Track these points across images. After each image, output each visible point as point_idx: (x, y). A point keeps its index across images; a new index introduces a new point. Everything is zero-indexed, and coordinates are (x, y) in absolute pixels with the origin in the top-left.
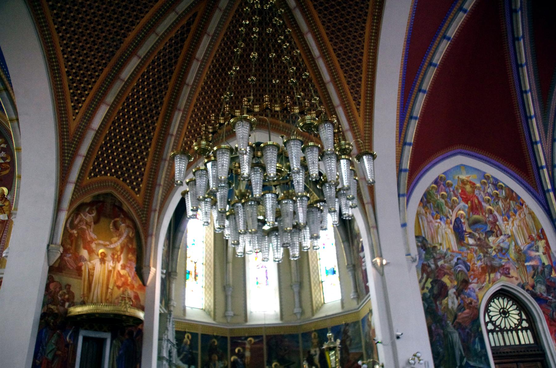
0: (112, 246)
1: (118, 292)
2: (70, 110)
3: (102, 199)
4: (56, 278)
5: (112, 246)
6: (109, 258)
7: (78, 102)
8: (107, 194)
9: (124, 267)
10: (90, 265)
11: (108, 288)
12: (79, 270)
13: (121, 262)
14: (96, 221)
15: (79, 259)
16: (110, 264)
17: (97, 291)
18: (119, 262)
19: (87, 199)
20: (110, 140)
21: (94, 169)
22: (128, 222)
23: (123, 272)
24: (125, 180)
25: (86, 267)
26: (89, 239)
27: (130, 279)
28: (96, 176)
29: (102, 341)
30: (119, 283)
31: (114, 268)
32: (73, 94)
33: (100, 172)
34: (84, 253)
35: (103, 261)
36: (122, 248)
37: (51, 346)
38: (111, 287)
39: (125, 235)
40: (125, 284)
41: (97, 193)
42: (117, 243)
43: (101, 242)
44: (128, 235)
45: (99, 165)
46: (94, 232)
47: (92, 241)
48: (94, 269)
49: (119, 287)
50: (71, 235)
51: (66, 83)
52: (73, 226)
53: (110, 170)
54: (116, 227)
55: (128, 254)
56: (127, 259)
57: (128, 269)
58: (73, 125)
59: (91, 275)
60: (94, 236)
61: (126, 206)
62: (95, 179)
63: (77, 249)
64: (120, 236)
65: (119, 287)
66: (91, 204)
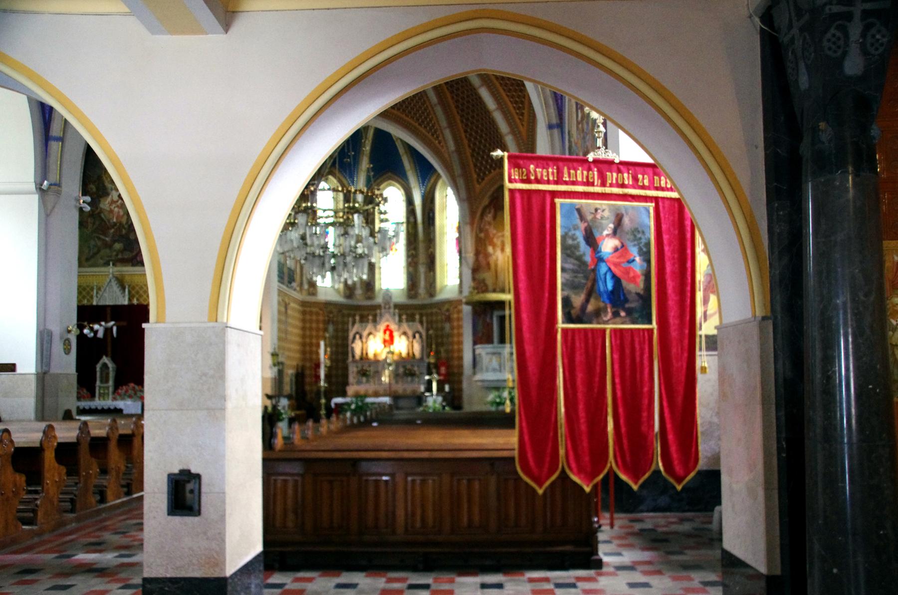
7: (437, 137)
10: (494, 257)
12: (488, 264)
15: (487, 255)
19: (486, 201)
20: (475, 144)
21: (478, 175)
25: (492, 260)
28: (483, 179)
32: (433, 135)
33: (484, 173)
34: (490, 249)
37: (480, 327)
41: (489, 193)
45: (480, 169)
47: (494, 235)
50: (481, 239)
51: (424, 131)
52: (481, 230)
58: (446, 156)
59: (496, 265)
60: (495, 232)
62: (484, 182)
63: (485, 249)
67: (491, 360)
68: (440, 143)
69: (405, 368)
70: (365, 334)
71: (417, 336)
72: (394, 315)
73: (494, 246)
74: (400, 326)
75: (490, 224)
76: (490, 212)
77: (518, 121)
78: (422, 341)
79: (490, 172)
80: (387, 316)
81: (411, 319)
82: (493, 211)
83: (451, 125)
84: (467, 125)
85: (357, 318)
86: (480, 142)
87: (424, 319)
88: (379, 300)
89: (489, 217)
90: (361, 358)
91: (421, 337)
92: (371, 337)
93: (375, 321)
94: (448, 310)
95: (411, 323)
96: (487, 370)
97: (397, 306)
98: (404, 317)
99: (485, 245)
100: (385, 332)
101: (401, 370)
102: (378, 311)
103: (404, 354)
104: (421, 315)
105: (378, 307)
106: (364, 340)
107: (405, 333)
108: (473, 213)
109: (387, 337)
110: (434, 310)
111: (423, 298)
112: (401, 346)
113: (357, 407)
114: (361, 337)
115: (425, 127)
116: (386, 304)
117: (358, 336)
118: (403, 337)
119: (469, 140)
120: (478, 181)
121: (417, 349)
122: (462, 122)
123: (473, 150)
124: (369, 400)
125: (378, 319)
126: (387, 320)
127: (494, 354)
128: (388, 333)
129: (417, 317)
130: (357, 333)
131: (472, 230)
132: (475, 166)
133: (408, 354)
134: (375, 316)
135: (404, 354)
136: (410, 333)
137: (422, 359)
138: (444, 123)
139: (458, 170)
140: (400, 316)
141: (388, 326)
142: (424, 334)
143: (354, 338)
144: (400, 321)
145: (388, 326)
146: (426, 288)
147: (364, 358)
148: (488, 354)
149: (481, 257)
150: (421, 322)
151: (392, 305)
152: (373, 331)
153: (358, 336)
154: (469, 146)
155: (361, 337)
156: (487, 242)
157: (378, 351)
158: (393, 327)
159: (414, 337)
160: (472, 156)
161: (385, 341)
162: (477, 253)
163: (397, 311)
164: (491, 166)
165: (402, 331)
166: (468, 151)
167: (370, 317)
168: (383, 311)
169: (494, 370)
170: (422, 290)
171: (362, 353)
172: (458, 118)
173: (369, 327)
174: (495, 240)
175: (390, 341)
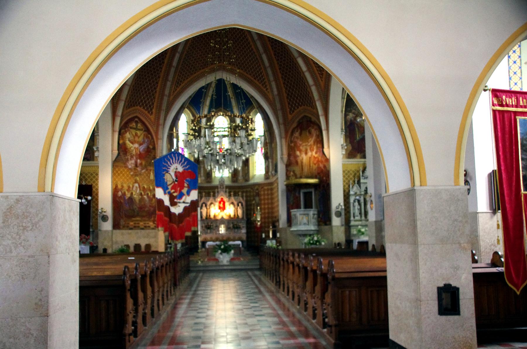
0: (309, 144)
1: (315, 167)
2: (266, 92)
3: (301, 121)
4: (289, 169)
5: (309, 144)
6: (309, 150)
7: (266, 86)
8: (303, 118)
9: (316, 153)
10: (301, 158)
11: (310, 166)
12: (297, 163)
13: (315, 151)
14: (301, 134)
15: (296, 157)
16: (310, 154)
17: (306, 169)
18: (313, 151)
19: (295, 125)
21: (291, 109)
22: (316, 127)
23: (316, 156)
24: (307, 105)
26: (299, 145)
27: (320, 158)
28: (293, 112)
29: (311, 192)
30: (315, 162)
31: (312, 155)
32: (263, 85)
33: (294, 109)
34: (298, 153)
35: (306, 153)
36: (314, 143)
38: (311, 165)
39: (315, 135)
40: (318, 161)
41: (298, 120)
42: (311, 141)
43: (304, 144)
44: (316, 135)
45: (292, 106)
46: (300, 141)
47: (300, 145)
48: (303, 159)
49: (315, 164)
51: (257, 83)
52: (291, 142)
53: (299, 104)
54: (310, 133)
55: (317, 144)
56: (317, 148)
57: (318, 153)
58: (271, 97)
59: (302, 162)
60: (301, 143)
61: (314, 119)
64: (312, 137)
65: (315, 164)
66: (297, 127)
67: (303, 218)
68: (267, 90)
69: (232, 224)
70: (208, 203)
71: (240, 204)
72: (226, 192)
73: (300, 151)
74: (229, 199)
75: (297, 138)
76: (297, 131)
77: (319, 79)
78: (243, 208)
79: (298, 108)
80: (222, 193)
81: (235, 195)
82: (299, 131)
83: (276, 80)
84: (285, 80)
85: (204, 194)
86: (293, 90)
87: (244, 194)
88: (216, 183)
89: (297, 134)
90: (206, 218)
91: (242, 205)
92: (212, 205)
93: (214, 196)
94: (257, 189)
95: (236, 197)
96: (300, 224)
97: (227, 187)
98: (232, 193)
99: (295, 151)
100: (220, 203)
101: (231, 226)
102: (216, 190)
103: (232, 216)
104: (243, 192)
105: (216, 187)
106: (208, 207)
107: (233, 203)
108: (286, 132)
109: (222, 205)
110: (249, 189)
111: (241, 181)
112: (230, 211)
113: (225, 247)
114: (206, 206)
115: (258, 80)
116: (221, 186)
117: (204, 205)
118: (232, 206)
119: (286, 89)
120: (290, 113)
121: (240, 212)
122: (282, 78)
123: (288, 95)
124: (231, 243)
125: (216, 194)
126: (222, 195)
127: (304, 214)
128: (222, 203)
129: (240, 193)
130: (204, 203)
131: (286, 141)
132: (289, 104)
133: (235, 215)
134: (214, 193)
135: (232, 216)
136: (236, 203)
137: (243, 218)
138: (271, 78)
139: (278, 106)
140: (230, 192)
141: (222, 199)
142: (244, 204)
143: (202, 206)
144: (230, 196)
145: (222, 199)
146: (243, 176)
147: (208, 217)
148: (300, 214)
149: (292, 158)
150: (242, 197)
151: (224, 186)
152: (213, 202)
153: (204, 205)
154: (286, 92)
155: (206, 206)
156: (296, 149)
157: (217, 214)
158: (225, 199)
159: (238, 205)
160: (287, 98)
161: (220, 208)
162: (289, 155)
163: (227, 190)
164: (299, 104)
165: (231, 201)
166: (285, 95)
167: (212, 194)
168: (219, 190)
169: (305, 224)
170: (240, 177)
171: (207, 215)
172: (280, 75)
173: (211, 199)
174: (301, 148)
175: (223, 208)
